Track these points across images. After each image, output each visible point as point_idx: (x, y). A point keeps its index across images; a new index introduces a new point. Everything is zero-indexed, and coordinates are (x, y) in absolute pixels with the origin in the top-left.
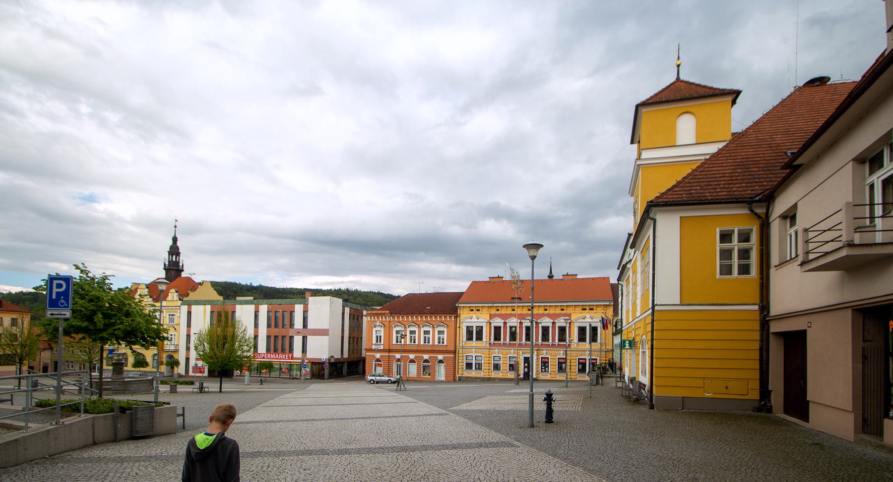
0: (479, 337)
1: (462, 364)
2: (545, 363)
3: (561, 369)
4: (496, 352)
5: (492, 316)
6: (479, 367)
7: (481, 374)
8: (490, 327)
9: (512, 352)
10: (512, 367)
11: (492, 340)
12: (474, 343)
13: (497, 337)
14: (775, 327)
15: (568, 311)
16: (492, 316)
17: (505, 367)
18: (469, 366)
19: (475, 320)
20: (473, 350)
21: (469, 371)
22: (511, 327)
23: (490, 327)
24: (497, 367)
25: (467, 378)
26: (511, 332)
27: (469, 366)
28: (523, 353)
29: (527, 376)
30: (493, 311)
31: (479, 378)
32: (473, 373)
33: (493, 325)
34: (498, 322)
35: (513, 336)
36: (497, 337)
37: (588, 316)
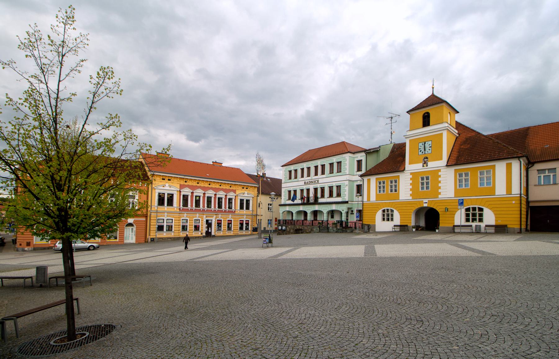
0: (170, 203)
1: (154, 227)
2: (219, 224)
3: (229, 228)
4: (185, 216)
5: (182, 187)
6: (170, 228)
7: (172, 235)
8: (180, 195)
9: (197, 216)
10: (197, 228)
11: (181, 206)
12: (166, 208)
13: (185, 203)
14: (531, 205)
15: (233, 188)
16: (182, 187)
17: (191, 228)
18: (160, 228)
19: (168, 188)
20: (166, 214)
21: (161, 232)
22: (196, 196)
23: (180, 195)
24: (184, 228)
25: (159, 238)
26: (196, 200)
27: (160, 228)
28: (206, 217)
29: (208, 234)
30: (182, 182)
31: (170, 238)
32: (164, 234)
33: (182, 194)
34: (187, 191)
35: (197, 203)
36: (185, 203)
37: (246, 193)
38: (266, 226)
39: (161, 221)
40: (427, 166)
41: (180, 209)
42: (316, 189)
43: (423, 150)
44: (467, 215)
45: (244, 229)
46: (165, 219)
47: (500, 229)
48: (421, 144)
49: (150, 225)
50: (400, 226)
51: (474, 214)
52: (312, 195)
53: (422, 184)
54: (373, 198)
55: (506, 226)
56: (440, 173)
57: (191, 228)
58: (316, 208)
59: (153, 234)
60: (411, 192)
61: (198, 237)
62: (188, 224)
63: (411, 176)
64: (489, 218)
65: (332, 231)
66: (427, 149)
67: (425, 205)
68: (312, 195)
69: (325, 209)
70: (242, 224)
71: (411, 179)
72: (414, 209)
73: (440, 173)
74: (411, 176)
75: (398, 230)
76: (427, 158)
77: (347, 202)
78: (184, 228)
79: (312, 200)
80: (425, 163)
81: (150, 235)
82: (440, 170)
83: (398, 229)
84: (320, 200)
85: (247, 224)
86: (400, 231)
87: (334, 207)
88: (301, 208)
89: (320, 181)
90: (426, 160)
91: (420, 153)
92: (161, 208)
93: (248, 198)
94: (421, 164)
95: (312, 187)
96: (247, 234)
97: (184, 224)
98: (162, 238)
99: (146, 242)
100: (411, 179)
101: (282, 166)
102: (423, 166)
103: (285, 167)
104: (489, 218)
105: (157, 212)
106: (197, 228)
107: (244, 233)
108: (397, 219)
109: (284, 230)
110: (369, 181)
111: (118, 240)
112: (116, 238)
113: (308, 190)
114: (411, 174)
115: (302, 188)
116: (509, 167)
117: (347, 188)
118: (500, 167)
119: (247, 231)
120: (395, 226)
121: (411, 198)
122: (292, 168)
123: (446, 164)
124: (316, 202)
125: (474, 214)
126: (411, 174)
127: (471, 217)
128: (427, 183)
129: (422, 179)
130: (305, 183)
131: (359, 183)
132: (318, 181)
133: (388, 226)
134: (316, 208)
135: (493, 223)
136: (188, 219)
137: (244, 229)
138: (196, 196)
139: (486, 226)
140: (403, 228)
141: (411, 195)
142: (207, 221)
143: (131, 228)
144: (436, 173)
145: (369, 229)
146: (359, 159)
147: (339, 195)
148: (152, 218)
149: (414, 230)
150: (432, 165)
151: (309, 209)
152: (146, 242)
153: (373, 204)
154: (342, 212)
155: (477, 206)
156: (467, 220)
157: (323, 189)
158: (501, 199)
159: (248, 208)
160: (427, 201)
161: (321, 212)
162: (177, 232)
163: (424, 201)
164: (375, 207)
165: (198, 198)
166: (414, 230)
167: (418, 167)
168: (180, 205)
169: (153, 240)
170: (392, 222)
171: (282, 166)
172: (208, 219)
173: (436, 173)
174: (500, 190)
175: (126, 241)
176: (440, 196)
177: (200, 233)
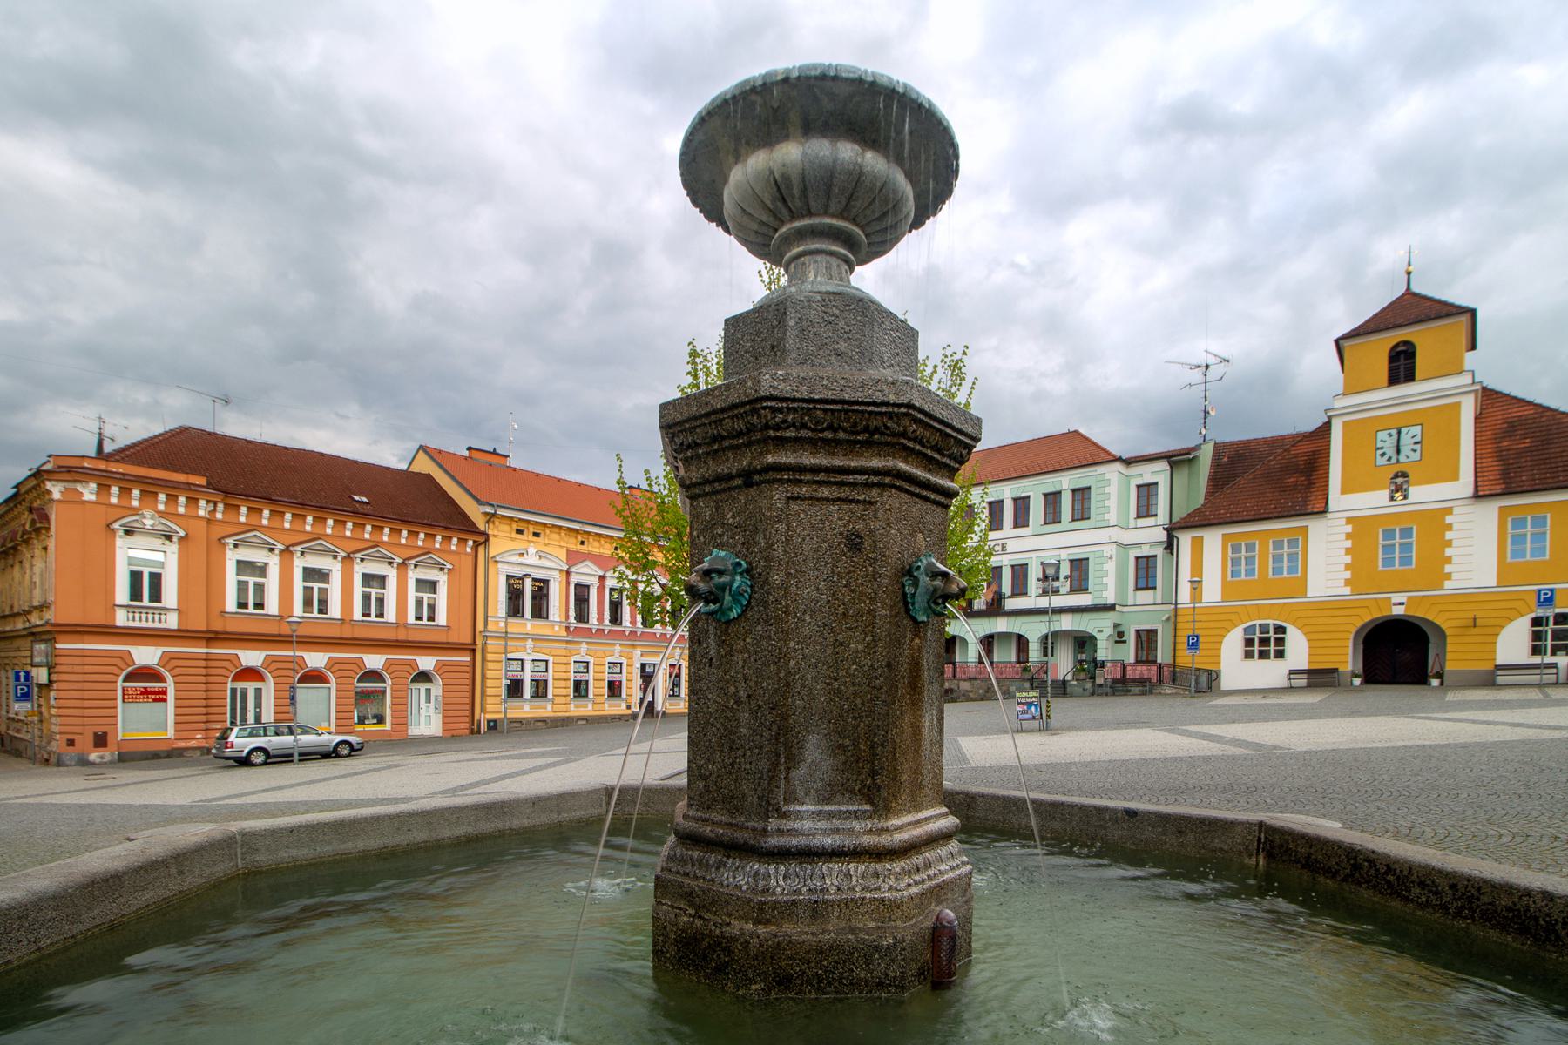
4: (583, 650)
6: (540, 689)
7: (547, 709)
8: (568, 583)
9: (616, 652)
10: (614, 689)
11: (572, 620)
12: (528, 624)
17: (597, 688)
20: (532, 645)
23: (568, 583)
24: (580, 689)
25: (512, 721)
26: (611, 602)
27: (515, 689)
31: (543, 720)
33: (575, 579)
39: (515, 666)
40: (1405, 497)
41: (567, 628)
43: (1391, 452)
46: (528, 658)
48: (1382, 435)
49: (484, 677)
50: (1309, 672)
53: (1388, 549)
57: (597, 688)
59: (495, 706)
61: (620, 718)
62: (591, 677)
66: (1405, 450)
67: (1398, 611)
72: (1359, 624)
75: (1303, 682)
76: (1404, 475)
78: (580, 689)
81: (483, 710)
83: (1301, 681)
86: (1309, 686)
90: (1399, 480)
91: (1382, 461)
92: (515, 626)
94: (1385, 493)
97: (580, 677)
98: (520, 721)
99: (474, 731)
102: (1392, 498)
105: (506, 636)
106: (614, 689)
111: (388, 726)
112: (380, 719)
114: (1349, 520)
120: (1292, 672)
121: (1347, 590)
126: (1349, 520)
129: (1389, 534)
133: (1271, 673)
136: (592, 661)
138: (612, 589)
140: (1319, 677)
142: (643, 666)
143: (423, 686)
148: (489, 657)
149: (1357, 682)
150: (1422, 495)
152: (472, 732)
160: (1404, 600)
162: (560, 703)
163: (1394, 600)
165: (616, 595)
166: (1357, 682)
167: (1375, 500)
168: (567, 617)
169: (493, 726)
172: (647, 660)
175: (414, 731)
177: (624, 706)
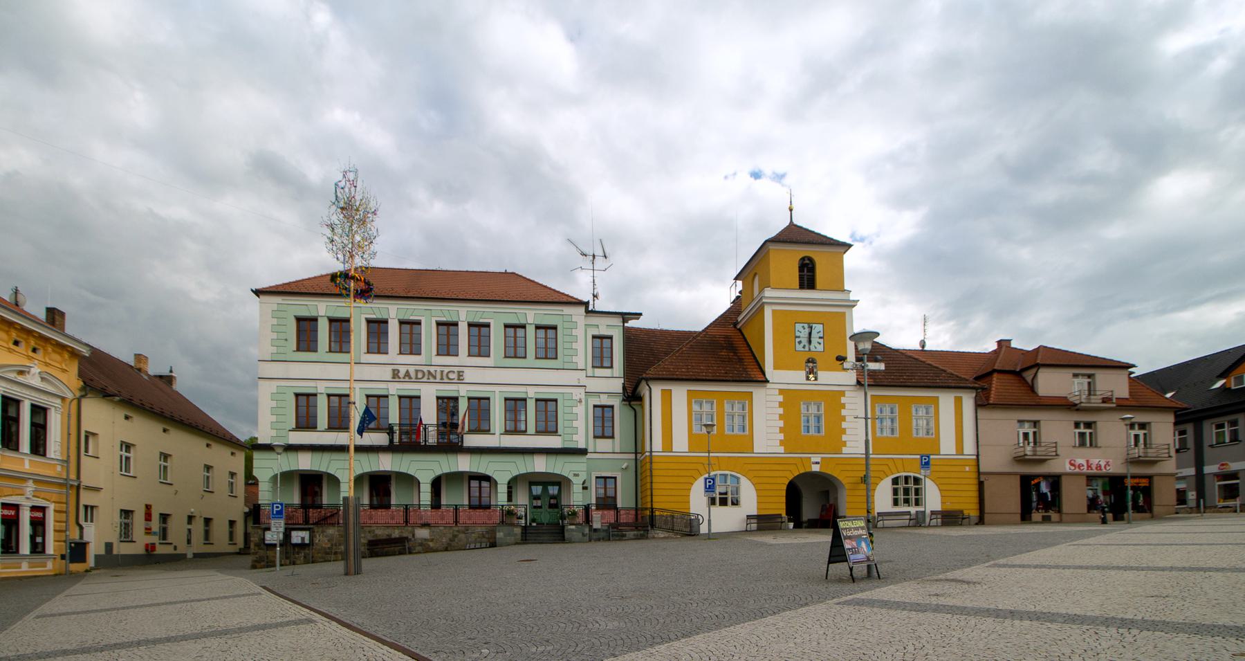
38: (113, 537)
42: (447, 404)
43: (805, 341)
44: (895, 492)
45: (25, 547)
47: (950, 518)
48: (799, 327)
51: (907, 490)
52: (429, 414)
54: (681, 443)
55: (962, 512)
56: (843, 400)
58: (464, 464)
60: (781, 436)
63: (781, 398)
64: (933, 500)
65: (578, 535)
66: (815, 340)
67: (816, 468)
68: (429, 414)
69: (502, 471)
70: (12, 524)
71: (781, 404)
73: (843, 400)
74: (781, 398)
75: (754, 526)
77: (583, 452)
79: (432, 439)
80: (811, 371)
82: (843, 393)
84: (471, 440)
85: (38, 525)
86: (759, 529)
87: (540, 465)
88: (386, 463)
89: (469, 375)
91: (799, 347)
93: (42, 400)
94: (803, 374)
95: (429, 395)
96: (38, 571)
100: (781, 404)
101: (258, 293)
102: (808, 378)
103: (264, 298)
104: (933, 500)
107: (25, 568)
108: (750, 502)
109: (302, 546)
110: (667, 396)
113: (410, 402)
114: (781, 392)
115: (378, 389)
116: (958, 401)
117: (580, 410)
118: (946, 400)
119: (38, 558)
120: (749, 517)
121: (781, 449)
122: (323, 308)
123: (854, 382)
124: (449, 445)
125: (907, 490)
126: (781, 392)
127: (901, 497)
128: (818, 418)
130: (395, 374)
131: (604, 400)
132: (460, 374)
133: (726, 520)
134: (464, 464)
135: (938, 508)
137: (25, 547)
139: (933, 513)
140: (764, 522)
141: (782, 443)
144: (833, 399)
145: (687, 528)
146: (604, 331)
147: (548, 428)
151: (425, 468)
153: (680, 460)
154: (574, 480)
155: (912, 474)
156: (896, 503)
157: (480, 405)
158: (948, 462)
159: (38, 446)
160: (818, 460)
161: (409, 481)
163: (813, 460)
164: (685, 470)
167: (796, 378)
170: (735, 508)
171: (258, 293)
173: (833, 399)
174: (947, 446)
176: (845, 450)
